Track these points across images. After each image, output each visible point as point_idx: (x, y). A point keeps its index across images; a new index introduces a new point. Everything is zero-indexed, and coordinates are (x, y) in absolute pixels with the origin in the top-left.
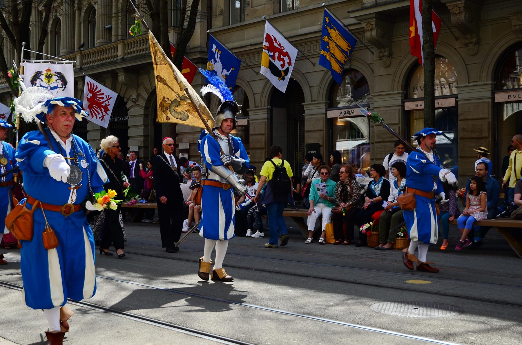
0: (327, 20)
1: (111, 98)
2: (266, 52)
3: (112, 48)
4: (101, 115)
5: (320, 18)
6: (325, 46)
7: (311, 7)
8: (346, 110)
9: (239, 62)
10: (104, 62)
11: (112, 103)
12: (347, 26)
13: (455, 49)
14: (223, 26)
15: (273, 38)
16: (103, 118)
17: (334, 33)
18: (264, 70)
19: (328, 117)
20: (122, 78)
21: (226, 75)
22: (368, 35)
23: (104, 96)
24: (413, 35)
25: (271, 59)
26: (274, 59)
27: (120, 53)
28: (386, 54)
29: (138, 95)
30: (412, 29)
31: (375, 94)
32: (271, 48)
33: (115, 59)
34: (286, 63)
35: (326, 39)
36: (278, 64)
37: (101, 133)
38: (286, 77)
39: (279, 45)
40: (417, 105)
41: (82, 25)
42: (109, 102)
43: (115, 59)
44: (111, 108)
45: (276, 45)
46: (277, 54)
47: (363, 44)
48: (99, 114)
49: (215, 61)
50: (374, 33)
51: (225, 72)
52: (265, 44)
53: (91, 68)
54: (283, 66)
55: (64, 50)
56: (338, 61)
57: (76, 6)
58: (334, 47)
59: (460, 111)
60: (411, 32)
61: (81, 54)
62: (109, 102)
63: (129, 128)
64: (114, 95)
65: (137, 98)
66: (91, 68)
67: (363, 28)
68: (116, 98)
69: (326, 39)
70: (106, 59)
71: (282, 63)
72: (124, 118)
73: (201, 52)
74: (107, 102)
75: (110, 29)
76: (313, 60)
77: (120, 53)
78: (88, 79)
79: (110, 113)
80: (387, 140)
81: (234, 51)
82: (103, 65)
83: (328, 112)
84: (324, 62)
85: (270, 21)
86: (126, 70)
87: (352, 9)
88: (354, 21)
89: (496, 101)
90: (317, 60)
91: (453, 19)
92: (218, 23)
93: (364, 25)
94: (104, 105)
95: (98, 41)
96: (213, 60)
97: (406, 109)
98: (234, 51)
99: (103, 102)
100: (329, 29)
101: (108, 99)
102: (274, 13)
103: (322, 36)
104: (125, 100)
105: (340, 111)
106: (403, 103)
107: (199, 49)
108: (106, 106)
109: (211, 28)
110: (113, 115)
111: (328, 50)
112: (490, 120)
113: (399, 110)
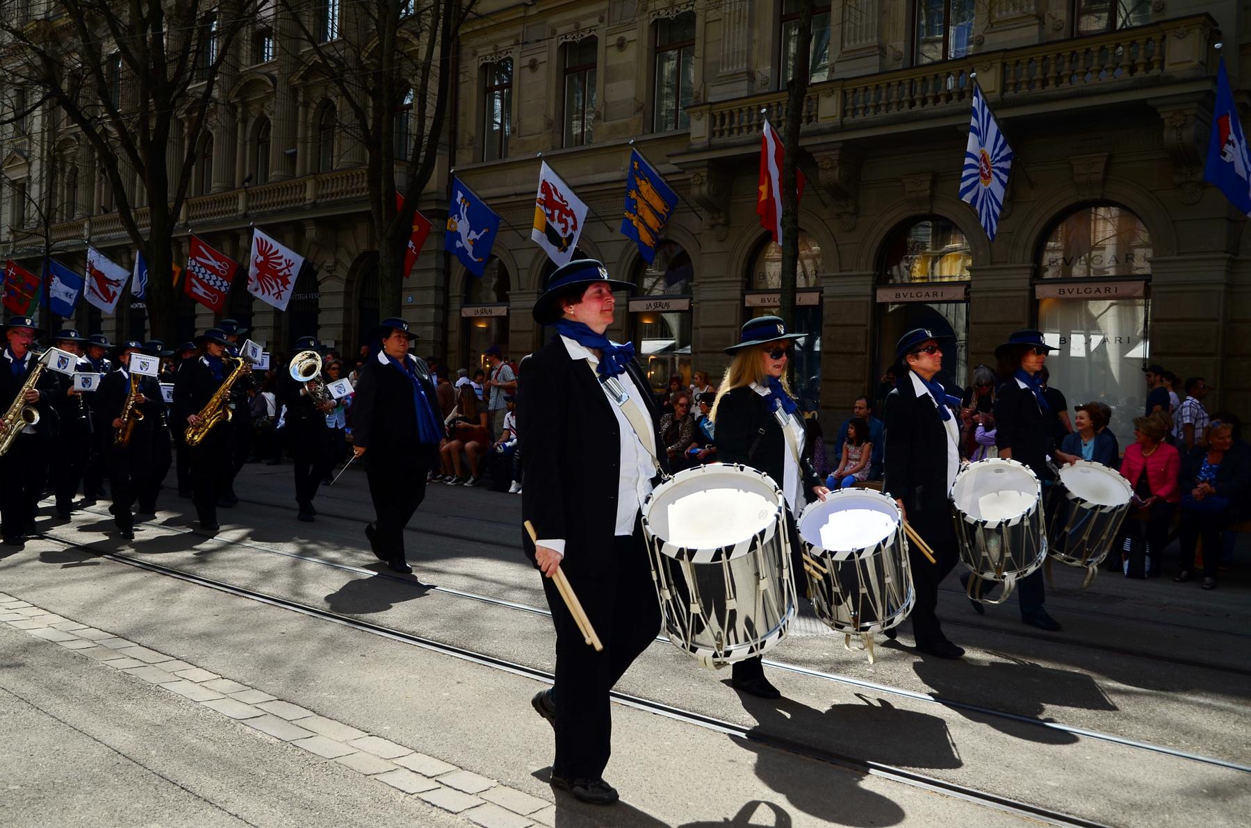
0: (636, 166)
1: (293, 264)
2: (543, 207)
3: (296, 186)
4: (276, 290)
5: (626, 161)
6: (631, 206)
7: (610, 143)
8: (658, 301)
9: (497, 219)
10: (283, 207)
11: (295, 271)
12: (663, 175)
13: (822, 220)
14: (474, 162)
15: (552, 187)
16: (280, 294)
17: (644, 187)
18: (536, 234)
19: (631, 310)
20: (311, 233)
21: (475, 240)
22: (695, 191)
23: (282, 260)
24: (764, 197)
25: (548, 218)
26: (553, 220)
27: (309, 194)
28: (721, 221)
29: (336, 262)
30: (763, 188)
31: (703, 280)
32: (549, 203)
33: (301, 204)
34: (570, 225)
35: (633, 195)
36: (558, 227)
37: (275, 317)
38: (569, 247)
39: (561, 198)
40: (763, 300)
41: (248, 147)
42: (289, 271)
43: (301, 204)
44: (292, 279)
45: (556, 198)
46: (557, 212)
47: (687, 203)
48: (273, 288)
49: (460, 218)
50: (704, 189)
51: (473, 235)
52: (540, 195)
53: (262, 215)
54: (565, 230)
55: (217, 184)
56: (649, 229)
57: (239, 116)
58: (645, 207)
59: (825, 313)
60: (760, 193)
61: (247, 192)
62: (289, 271)
63: (319, 311)
64: (298, 260)
65: (335, 266)
66: (262, 215)
67: (689, 179)
68: (301, 264)
69: (633, 195)
70: (287, 203)
71: (563, 225)
72: (312, 296)
73: (438, 201)
74: (286, 271)
75: (294, 156)
76: (610, 223)
77: (309, 194)
78: (258, 233)
79: (290, 287)
80: (718, 349)
81: (490, 202)
82: (282, 212)
83: (631, 303)
84: (629, 229)
85: (548, 159)
86: (318, 222)
87: (673, 150)
88: (676, 169)
89: (878, 300)
90: (618, 225)
91: (822, 176)
92: (465, 158)
93: (689, 175)
94: (281, 274)
95: (274, 173)
96: (456, 216)
97: (747, 305)
98: (490, 202)
99: (281, 270)
100: (638, 179)
101: (288, 266)
102: (553, 148)
103: (629, 188)
104: (315, 268)
105: (648, 302)
106: (743, 295)
107: (435, 196)
108: (286, 276)
109: (454, 165)
110: (295, 290)
111: (635, 212)
112: (869, 328)
113: (737, 305)
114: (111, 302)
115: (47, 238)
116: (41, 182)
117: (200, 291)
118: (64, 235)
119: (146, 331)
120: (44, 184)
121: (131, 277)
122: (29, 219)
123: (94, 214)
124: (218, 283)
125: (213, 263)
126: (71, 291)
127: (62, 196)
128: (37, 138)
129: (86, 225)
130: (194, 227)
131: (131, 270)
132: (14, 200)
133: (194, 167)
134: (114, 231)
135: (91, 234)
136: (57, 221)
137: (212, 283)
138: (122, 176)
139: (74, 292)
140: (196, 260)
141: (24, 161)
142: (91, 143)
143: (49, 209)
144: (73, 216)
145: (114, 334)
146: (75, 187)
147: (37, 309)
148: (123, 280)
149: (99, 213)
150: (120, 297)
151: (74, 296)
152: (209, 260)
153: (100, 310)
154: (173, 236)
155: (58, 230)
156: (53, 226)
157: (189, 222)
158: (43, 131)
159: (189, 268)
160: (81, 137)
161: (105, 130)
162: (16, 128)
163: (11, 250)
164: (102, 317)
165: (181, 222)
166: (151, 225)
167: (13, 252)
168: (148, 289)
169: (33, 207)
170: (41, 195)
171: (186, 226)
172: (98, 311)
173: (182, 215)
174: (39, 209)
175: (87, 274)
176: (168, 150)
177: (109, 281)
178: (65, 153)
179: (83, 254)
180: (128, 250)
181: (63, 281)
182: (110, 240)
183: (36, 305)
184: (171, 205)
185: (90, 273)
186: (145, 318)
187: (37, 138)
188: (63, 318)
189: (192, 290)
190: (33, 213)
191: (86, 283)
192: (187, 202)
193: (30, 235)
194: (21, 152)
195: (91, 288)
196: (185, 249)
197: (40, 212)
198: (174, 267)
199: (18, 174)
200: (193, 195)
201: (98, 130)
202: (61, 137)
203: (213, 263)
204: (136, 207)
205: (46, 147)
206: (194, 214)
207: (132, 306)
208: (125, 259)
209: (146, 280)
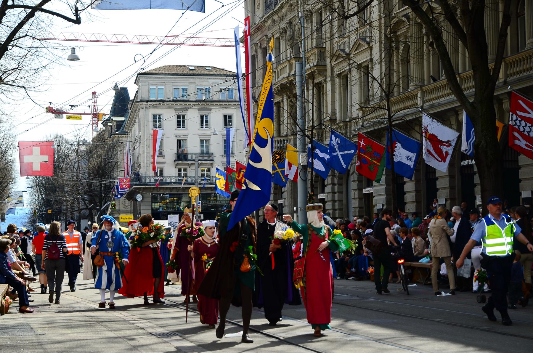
114: (444, 162)
115: (389, 110)
116: (381, 62)
117: (522, 143)
118: (402, 106)
119: (475, 185)
120: (383, 64)
121: (460, 137)
122: (373, 96)
123: (425, 83)
126: (411, 154)
127: (398, 72)
128: (376, 24)
129: (419, 95)
130: (512, 84)
131: (459, 130)
132: (361, 80)
133: (509, 27)
134: (443, 96)
135: (424, 102)
136: (395, 94)
138: (447, 46)
139: (413, 155)
140: (517, 115)
141: (366, 46)
142: (419, 21)
143: (389, 85)
144: (408, 88)
145: (448, 191)
146: (408, 62)
147: (384, 173)
148: (453, 141)
149: (429, 83)
150: (452, 156)
151: (413, 159)
152: (529, 113)
153: (435, 169)
154: (495, 94)
155: (398, 102)
156: (392, 99)
157: (508, 79)
158: (380, 19)
159: (510, 123)
160: (411, 17)
161: (430, 7)
162: (360, 18)
163: (361, 124)
164: (437, 175)
165: (501, 81)
166: (475, 87)
167: (363, 126)
168: (476, 146)
169: (376, 85)
170: (381, 73)
171: (505, 83)
172: (434, 170)
173: (501, 75)
174: (381, 85)
175: (424, 139)
176: (485, 16)
177: (441, 143)
178: (398, 33)
179: (418, 121)
180: (455, 112)
181: (404, 147)
182: (440, 105)
183: (383, 171)
184: (491, 66)
185: (426, 137)
186: (475, 174)
187: (376, 24)
188: (405, 179)
189: (514, 142)
190: (376, 89)
191: (424, 147)
192: (505, 62)
193: (375, 109)
194: (364, 39)
195: (428, 150)
196: (506, 105)
197: (382, 88)
198: (498, 124)
199: (362, 58)
200: (509, 54)
201: (425, 8)
202: (395, 20)
204: (460, 72)
205: (383, 31)
206: (511, 71)
207: (462, 164)
208: (453, 122)
209: (473, 139)
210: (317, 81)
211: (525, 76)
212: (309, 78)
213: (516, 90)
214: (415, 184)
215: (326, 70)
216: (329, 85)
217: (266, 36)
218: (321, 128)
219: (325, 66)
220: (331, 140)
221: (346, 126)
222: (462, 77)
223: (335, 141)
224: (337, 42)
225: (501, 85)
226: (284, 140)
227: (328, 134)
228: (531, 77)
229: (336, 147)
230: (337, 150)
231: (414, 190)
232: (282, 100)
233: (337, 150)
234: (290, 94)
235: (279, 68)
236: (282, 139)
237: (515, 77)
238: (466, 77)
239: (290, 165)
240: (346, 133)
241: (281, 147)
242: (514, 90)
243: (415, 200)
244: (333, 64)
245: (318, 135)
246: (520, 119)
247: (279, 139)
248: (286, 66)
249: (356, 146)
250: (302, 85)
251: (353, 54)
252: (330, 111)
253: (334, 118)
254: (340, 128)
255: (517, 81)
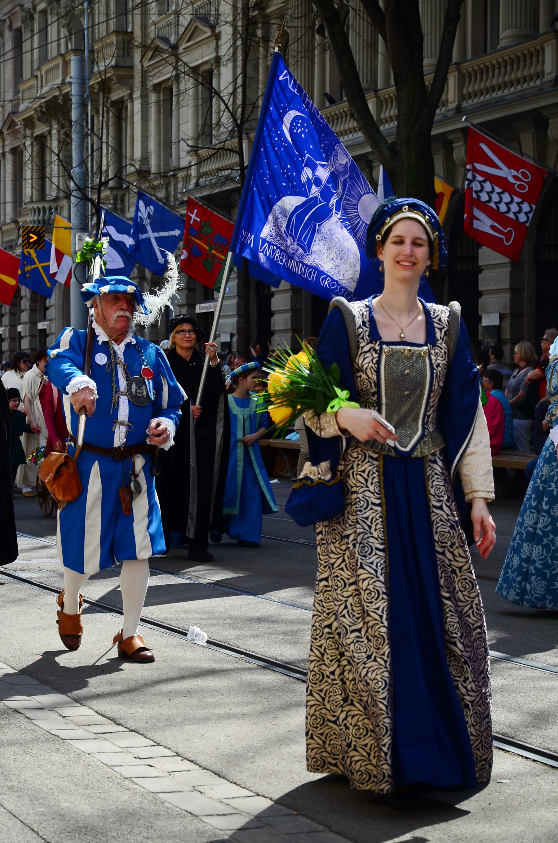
124: (514, 208)
125: (505, 172)
137: (503, 208)
141: (209, 33)
152: (498, 167)
157: (464, 104)
163: (193, 181)
167: (197, 184)
171: (459, 110)
178: (268, 11)
192: (459, 71)
194: (204, 19)
200: (469, 56)
203: (505, 172)
204: (379, 86)
206: (470, 90)
210: (114, 96)
211: (494, 98)
212: (100, 90)
213: (477, 124)
214: (292, 298)
215: (132, 77)
216: (137, 105)
217: (21, 6)
218: (120, 187)
219: (132, 68)
220: (138, 210)
221: (167, 185)
222: (382, 98)
223: (144, 212)
224: (154, 23)
225: (450, 114)
226: (50, 208)
227: (134, 200)
228: (505, 100)
229: (147, 222)
230: (149, 228)
231: (289, 308)
232: (50, 132)
233: (149, 228)
234: (63, 120)
235: (45, 68)
236: (47, 205)
237: (476, 100)
238: (389, 96)
239: (60, 256)
240: (167, 197)
241: (44, 220)
242: (473, 125)
243: (289, 327)
244: (146, 64)
245: (115, 200)
246: (481, 179)
247: (40, 206)
248: (57, 66)
249: (184, 223)
250: (83, 105)
251: (184, 47)
252: (138, 154)
253: (145, 168)
254: (155, 188)
255: (480, 107)
